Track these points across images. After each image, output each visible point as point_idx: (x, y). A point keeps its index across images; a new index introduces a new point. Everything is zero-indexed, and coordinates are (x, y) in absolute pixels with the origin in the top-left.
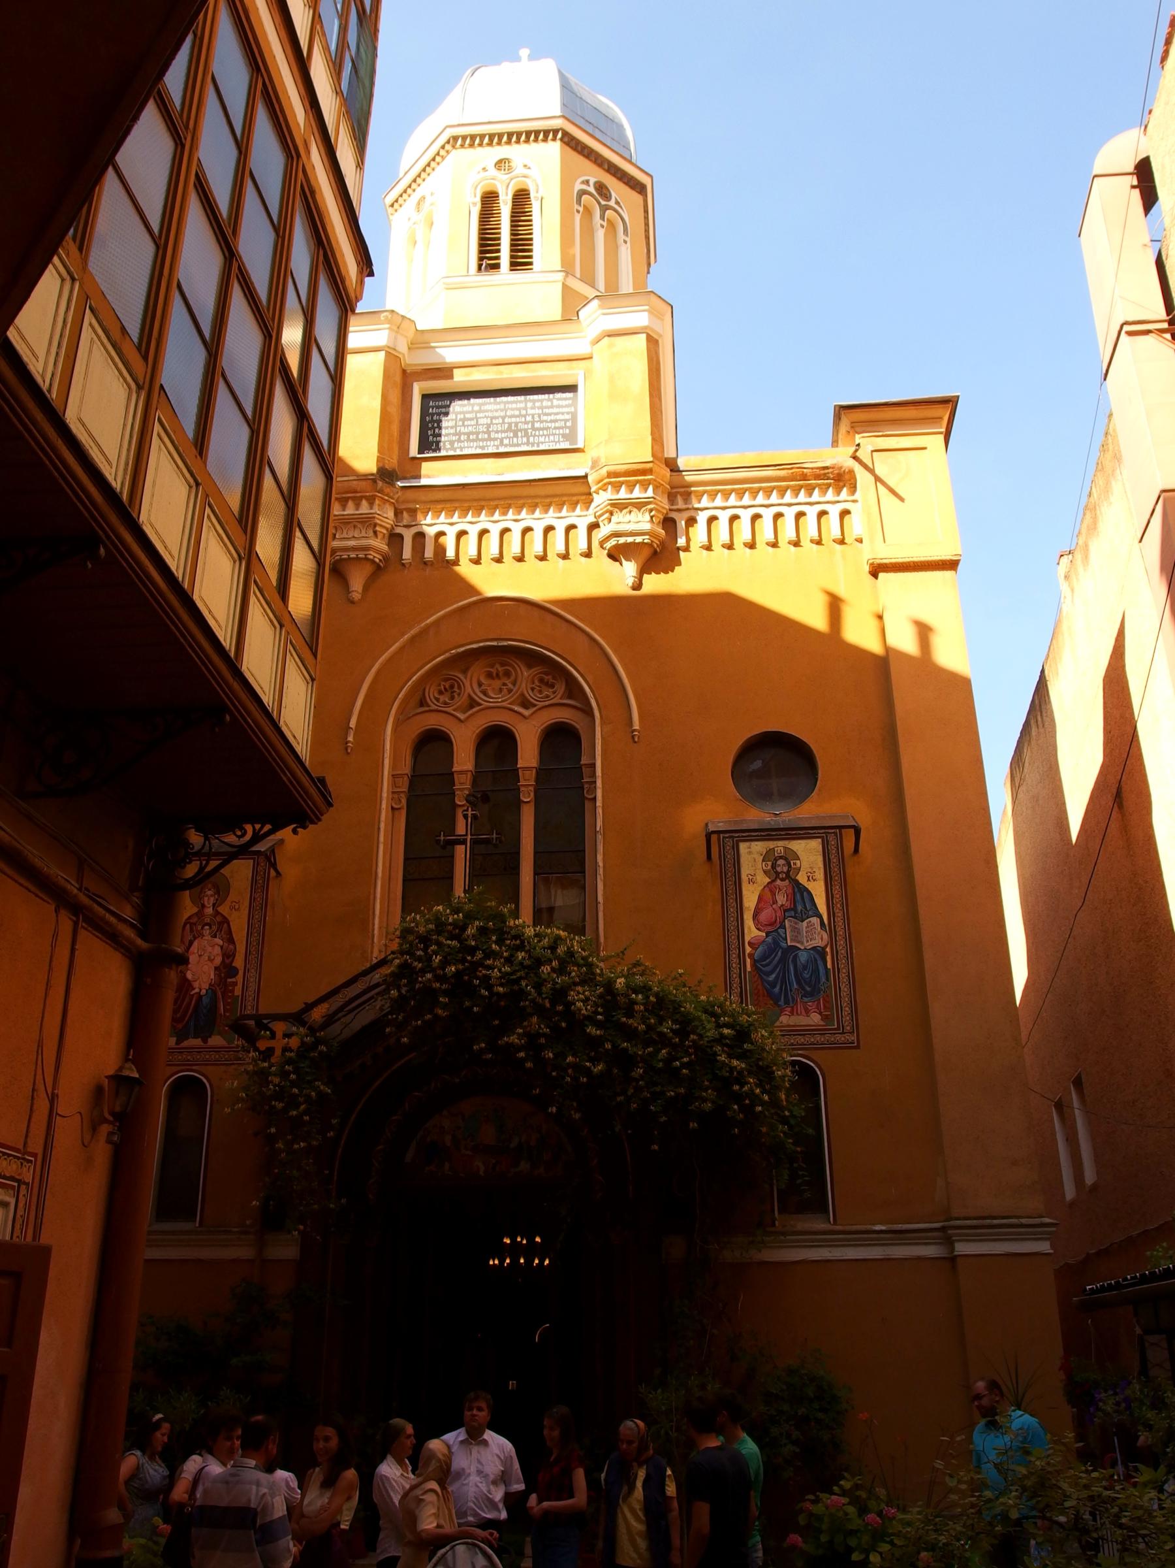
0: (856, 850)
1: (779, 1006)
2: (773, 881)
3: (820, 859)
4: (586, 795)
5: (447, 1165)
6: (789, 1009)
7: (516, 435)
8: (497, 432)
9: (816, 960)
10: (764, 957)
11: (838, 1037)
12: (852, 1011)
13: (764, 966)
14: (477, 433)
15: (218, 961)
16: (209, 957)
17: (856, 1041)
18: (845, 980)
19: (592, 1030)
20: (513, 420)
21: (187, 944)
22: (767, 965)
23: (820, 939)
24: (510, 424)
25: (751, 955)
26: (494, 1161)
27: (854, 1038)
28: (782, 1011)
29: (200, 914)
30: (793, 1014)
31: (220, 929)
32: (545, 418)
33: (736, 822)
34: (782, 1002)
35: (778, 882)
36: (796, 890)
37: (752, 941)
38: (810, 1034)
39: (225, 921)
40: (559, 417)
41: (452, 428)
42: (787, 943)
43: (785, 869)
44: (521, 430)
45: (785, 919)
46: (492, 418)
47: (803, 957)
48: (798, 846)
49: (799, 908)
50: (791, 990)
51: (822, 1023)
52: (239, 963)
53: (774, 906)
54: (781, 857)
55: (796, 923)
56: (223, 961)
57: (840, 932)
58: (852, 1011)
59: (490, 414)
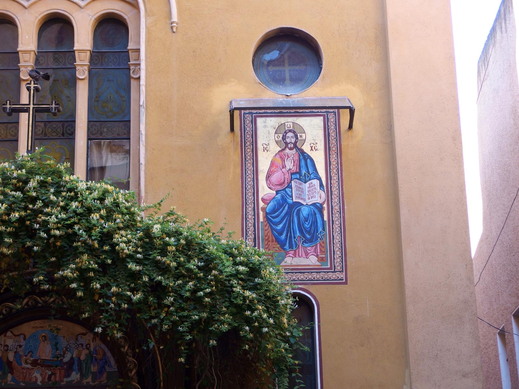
0: (350, 127)
1: (284, 250)
2: (283, 150)
3: (321, 133)
4: (132, 75)
5: (10, 376)
6: (292, 252)
10: (274, 211)
11: (330, 275)
12: (342, 254)
13: (274, 218)
17: (344, 278)
18: (338, 230)
19: (133, 266)
22: (277, 217)
23: (320, 197)
25: (263, 209)
26: (50, 373)
27: (343, 276)
28: (287, 253)
30: (295, 257)
33: (255, 101)
34: (287, 247)
35: (287, 151)
36: (301, 157)
37: (265, 197)
38: (309, 272)
42: (292, 200)
43: (293, 140)
45: (291, 180)
47: (305, 211)
48: (303, 122)
49: (304, 172)
50: (295, 237)
51: (320, 264)
53: (283, 170)
54: (290, 131)
55: (300, 184)
57: (335, 192)
58: (342, 254)
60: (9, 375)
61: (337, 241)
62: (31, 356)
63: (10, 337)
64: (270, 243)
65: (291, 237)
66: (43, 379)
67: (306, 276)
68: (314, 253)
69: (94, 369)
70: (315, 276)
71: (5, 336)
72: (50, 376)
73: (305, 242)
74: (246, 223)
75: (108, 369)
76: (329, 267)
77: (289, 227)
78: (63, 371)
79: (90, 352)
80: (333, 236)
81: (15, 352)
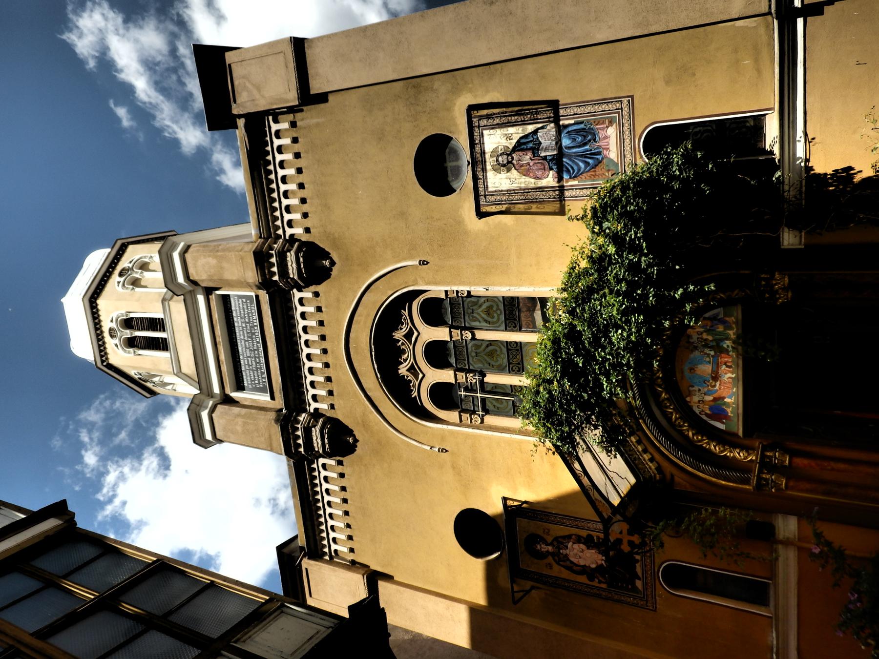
6: (605, 151)
7: (254, 334)
8: (253, 345)
9: (568, 132)
11: (625, 113)
12: (605, 103)
14: (255, 357)
15: (583, 546)
16: (581, 552)
17: (628, 99)
18: (582, 109)
20: (245, 335)
21: (572, 565)
24: (248, 337)
26: (724, 367)
27: (625, 100)
29: (552, 554)
30: (609, 148)
31: (562, 543)
32: (242, 315)
34: (600, 157)
38: (623, 135)
39: (556, 539)
40: (241, 305)
41: (254, 373)
43: (505, 157)
44: (251, 330)
46: (246, 348)
50: (591, 150)
51: (615, 124)
52: (584, 533)
53: (531, 164)
56: (584, 543)
58: (605, 103)
59: (244, 349)
60: (725, 400)
61: (592, 109)
62: (709, 381)
63: (691, 399)
64: (597, 173)
65: (590, 154)
66: (730, 372)
67: (627, 137)
68: (605, 131)
69: (721, 328)
70: (626, 128)
71: (690, 402)
72: (727, 366)
73: (594, 140)
74: (580, 197)
75: (721, 316)
76: (617, 115)
77: (584, 156)
78: (723, 355)
79: (705, 332)
80: (588, 113)
81: (705, 394)
